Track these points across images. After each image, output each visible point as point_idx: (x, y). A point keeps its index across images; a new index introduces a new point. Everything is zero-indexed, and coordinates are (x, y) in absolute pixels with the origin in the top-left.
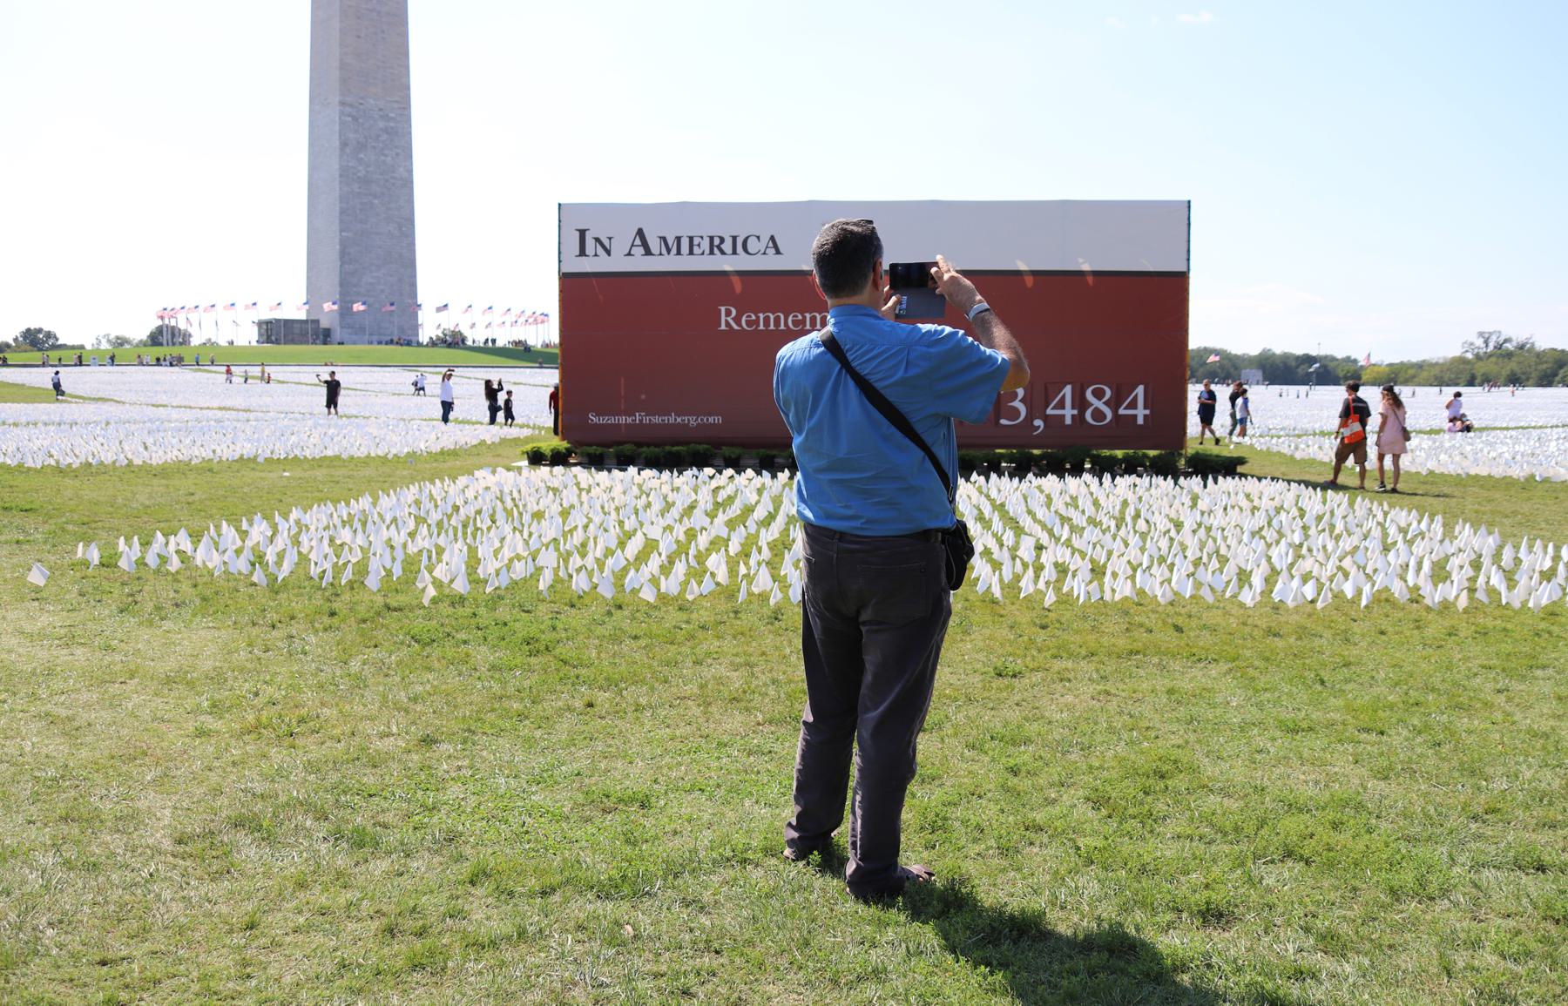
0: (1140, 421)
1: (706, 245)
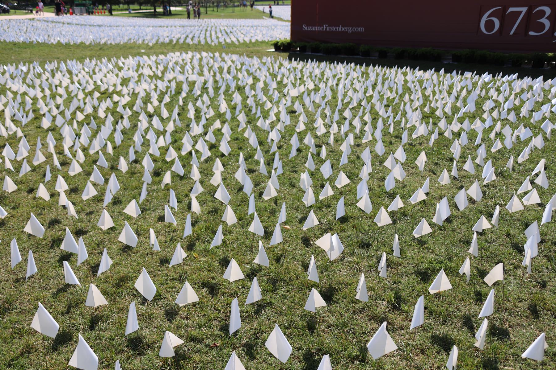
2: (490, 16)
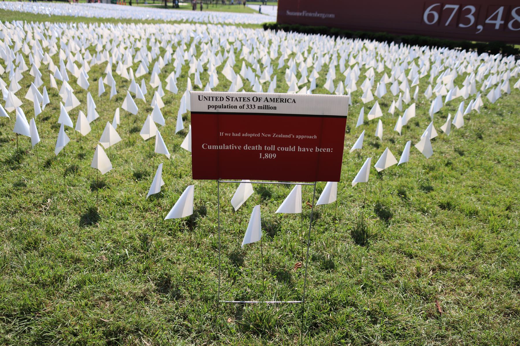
2: (431, 10)
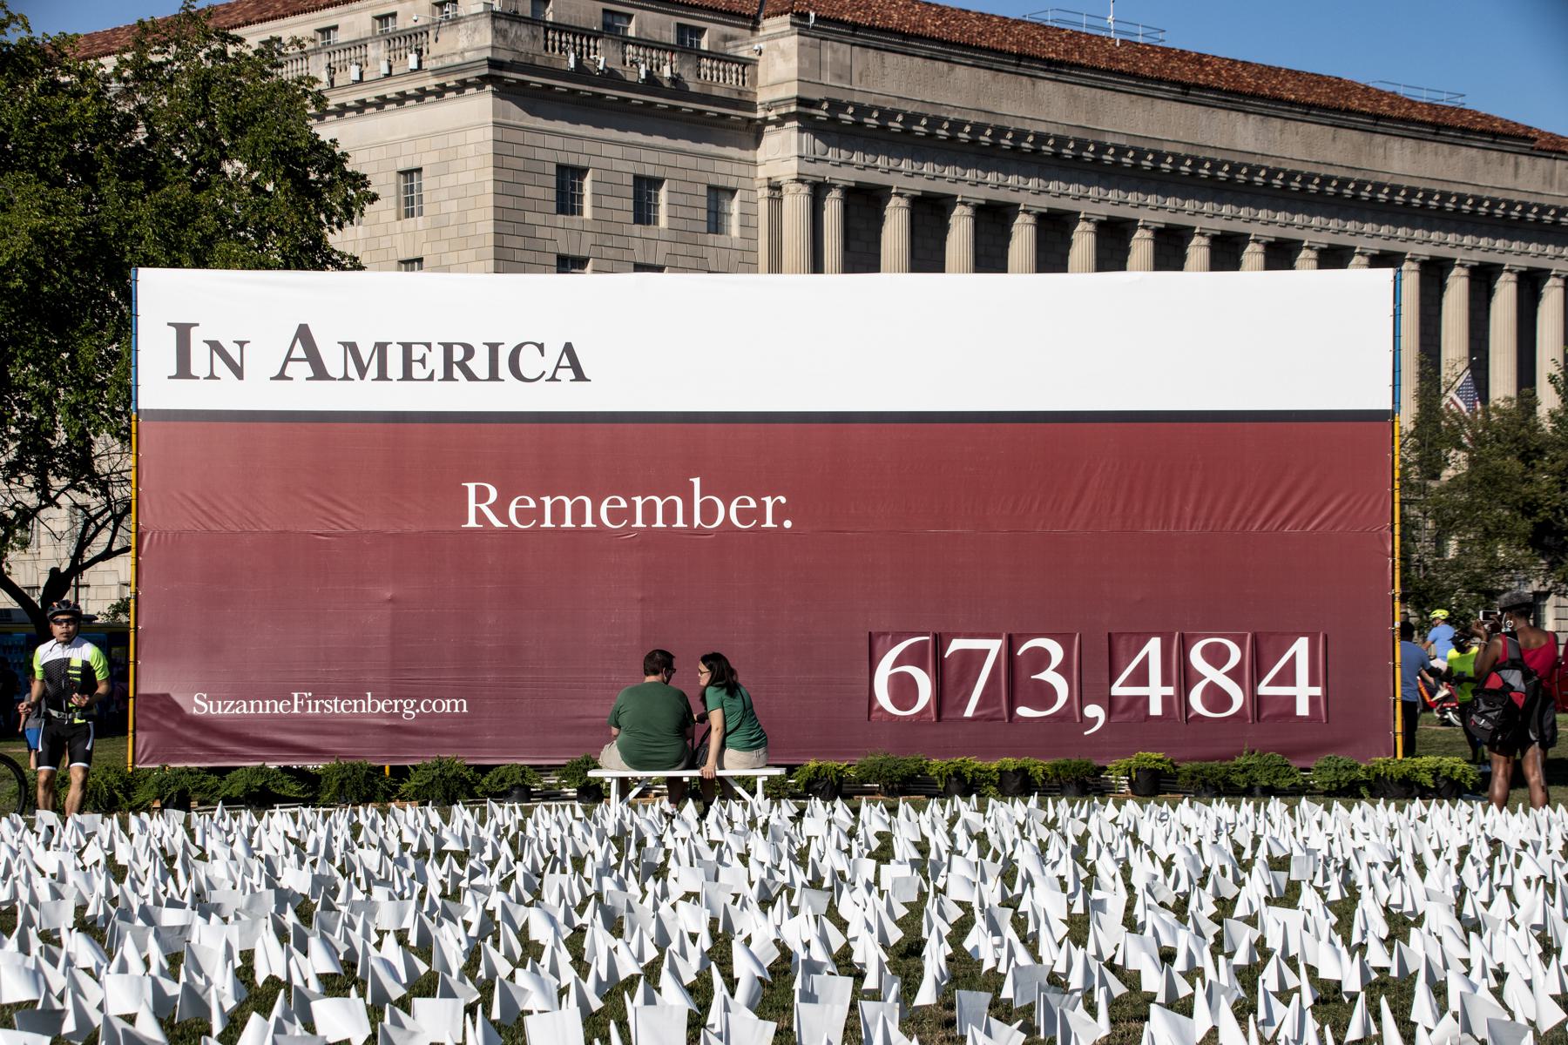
0: (1303, 709)
1: (436, 360)
2: (898, 662)
